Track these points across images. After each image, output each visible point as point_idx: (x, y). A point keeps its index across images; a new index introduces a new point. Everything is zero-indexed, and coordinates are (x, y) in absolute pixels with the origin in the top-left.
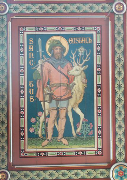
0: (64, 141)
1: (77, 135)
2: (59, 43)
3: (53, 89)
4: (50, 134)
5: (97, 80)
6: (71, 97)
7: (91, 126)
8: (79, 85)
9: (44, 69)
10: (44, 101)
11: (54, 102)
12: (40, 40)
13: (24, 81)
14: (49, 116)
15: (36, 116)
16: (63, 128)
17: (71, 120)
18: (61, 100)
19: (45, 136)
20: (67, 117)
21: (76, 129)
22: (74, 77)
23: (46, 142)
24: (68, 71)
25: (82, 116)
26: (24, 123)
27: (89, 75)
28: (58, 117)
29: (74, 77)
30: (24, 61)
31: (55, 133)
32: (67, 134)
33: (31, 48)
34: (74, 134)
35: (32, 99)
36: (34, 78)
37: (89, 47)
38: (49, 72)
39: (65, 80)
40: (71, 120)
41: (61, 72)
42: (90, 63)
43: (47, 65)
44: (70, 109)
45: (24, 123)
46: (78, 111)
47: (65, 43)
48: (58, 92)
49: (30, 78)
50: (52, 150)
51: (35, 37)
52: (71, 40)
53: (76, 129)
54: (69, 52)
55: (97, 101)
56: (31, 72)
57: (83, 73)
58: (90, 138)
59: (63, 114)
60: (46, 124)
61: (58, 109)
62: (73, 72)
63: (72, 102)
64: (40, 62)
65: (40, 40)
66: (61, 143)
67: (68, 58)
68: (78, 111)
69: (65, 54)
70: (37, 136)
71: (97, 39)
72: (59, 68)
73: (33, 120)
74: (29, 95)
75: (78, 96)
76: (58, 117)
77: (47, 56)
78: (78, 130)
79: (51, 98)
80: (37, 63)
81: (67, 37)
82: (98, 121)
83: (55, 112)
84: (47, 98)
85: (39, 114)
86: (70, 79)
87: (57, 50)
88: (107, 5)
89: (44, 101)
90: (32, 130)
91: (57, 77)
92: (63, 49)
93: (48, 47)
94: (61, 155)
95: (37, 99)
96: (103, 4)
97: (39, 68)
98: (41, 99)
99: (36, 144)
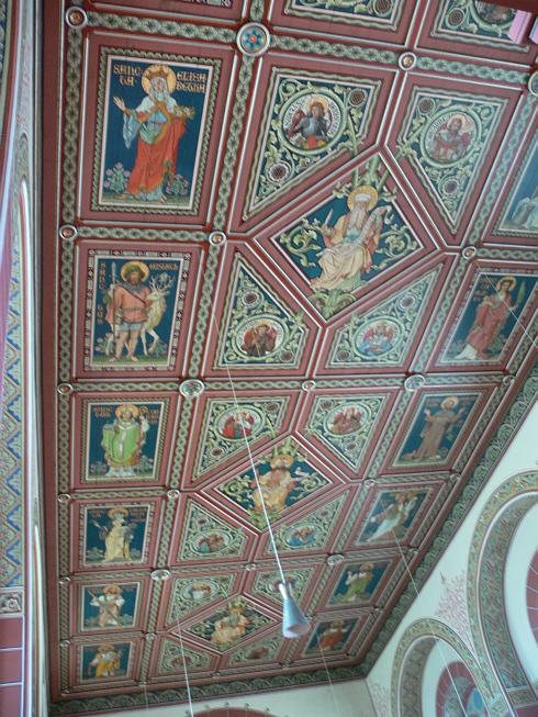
0: (135, 359)
1: (149, 353)
2: (138, 269)
3: (126, 313)
4: (119, 352)
5: (178, 305)
6: (146, 321)
7: (165, 346)
8: (157, 310)
9: (116, 294)
10: (114, 324)
11: (126, 324)
12: (114, 265)
13: (92, 304)
14: (118, 337)
15: (103, 337)
16: (134, 347)
17: (144, 341)
18: (134, 323)
19: (113, 354)
20: (140, 339)
21: (148, 347)
22: (151, 302)
23: (113, 360)
24: (146, 296)
25: (156, 337)
26: (90, 343)
27: (169, 301)
28: (129, 338)
29: (151, 302)
30: (93, 285)
31: (125, 351)
32: (139, 352)
33: (103, 272)
34: (145, 352)
35: (100, 322)
36: (104, 301)
37: (173, 274)
38: (123, 296)
39: (141, 305)
40: (144, 341)
41: (136, 297)
42: (173, 290)
43: (121, 290)
44: (143, 331)
45: (90, 343)
46: (153, 333)
47: (144, 269)
48: (130, 316)
49: (99, 301)
50: (120, 366)
51: (109, 262)
52: (153, 267)
53: (148, 347)
54: (149, 279)
55: (175, 325)
56: (99, 296)
57: (164, 300)
58: (163, 356)
59: (135, 335)
60: (115, 344)
61: (129, 332)
62: (151, 297)
63: (146, 325)
64: (112, 286)
65: (114, 265)
66: (131, 361)
67: (147, 284)
68: (153, 333)
69: (144, 280)
70: (104, 354)
71: (184, 266)
72: (135, 293)
73: (100, 340)
74: (97, 318)
75: (154, 319)
76: (129, 338)
77: (122, 281)
78: (151, 350)
79: (123, 320)
80: (108, 287)
81: (148, 263)
82: (173, 342)
83: (126, 334)
84: (118, 321)
85: (107, 335)
86: (147, 304)
87: (135, 276)
88: (202, 234)
89: (114, 324)
90: (98, 349)
91: (130, 301)
92: (142, 275)
93: (123, 271)
94: (129, 374)
95: (106, 322)
96: (198, 233)
97: (110, 293)
98: (110, 321)
99: (103, 361)
